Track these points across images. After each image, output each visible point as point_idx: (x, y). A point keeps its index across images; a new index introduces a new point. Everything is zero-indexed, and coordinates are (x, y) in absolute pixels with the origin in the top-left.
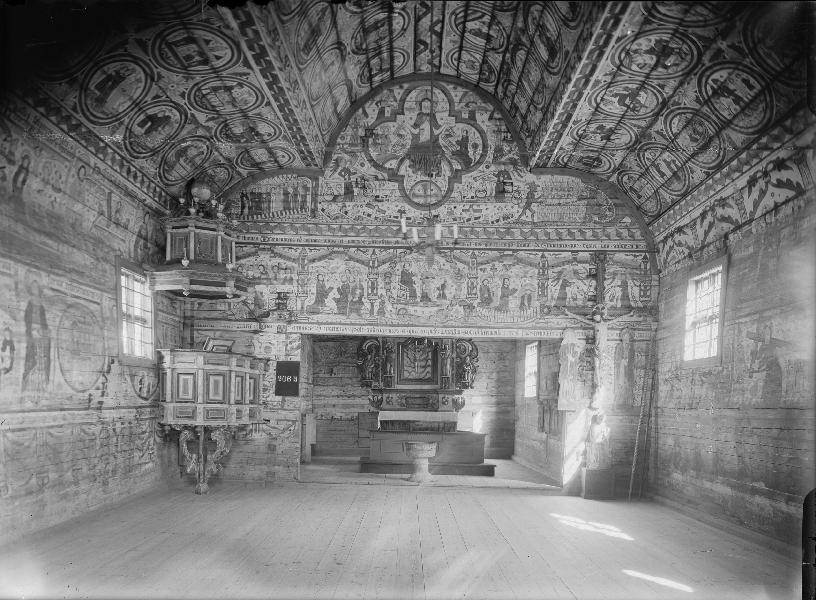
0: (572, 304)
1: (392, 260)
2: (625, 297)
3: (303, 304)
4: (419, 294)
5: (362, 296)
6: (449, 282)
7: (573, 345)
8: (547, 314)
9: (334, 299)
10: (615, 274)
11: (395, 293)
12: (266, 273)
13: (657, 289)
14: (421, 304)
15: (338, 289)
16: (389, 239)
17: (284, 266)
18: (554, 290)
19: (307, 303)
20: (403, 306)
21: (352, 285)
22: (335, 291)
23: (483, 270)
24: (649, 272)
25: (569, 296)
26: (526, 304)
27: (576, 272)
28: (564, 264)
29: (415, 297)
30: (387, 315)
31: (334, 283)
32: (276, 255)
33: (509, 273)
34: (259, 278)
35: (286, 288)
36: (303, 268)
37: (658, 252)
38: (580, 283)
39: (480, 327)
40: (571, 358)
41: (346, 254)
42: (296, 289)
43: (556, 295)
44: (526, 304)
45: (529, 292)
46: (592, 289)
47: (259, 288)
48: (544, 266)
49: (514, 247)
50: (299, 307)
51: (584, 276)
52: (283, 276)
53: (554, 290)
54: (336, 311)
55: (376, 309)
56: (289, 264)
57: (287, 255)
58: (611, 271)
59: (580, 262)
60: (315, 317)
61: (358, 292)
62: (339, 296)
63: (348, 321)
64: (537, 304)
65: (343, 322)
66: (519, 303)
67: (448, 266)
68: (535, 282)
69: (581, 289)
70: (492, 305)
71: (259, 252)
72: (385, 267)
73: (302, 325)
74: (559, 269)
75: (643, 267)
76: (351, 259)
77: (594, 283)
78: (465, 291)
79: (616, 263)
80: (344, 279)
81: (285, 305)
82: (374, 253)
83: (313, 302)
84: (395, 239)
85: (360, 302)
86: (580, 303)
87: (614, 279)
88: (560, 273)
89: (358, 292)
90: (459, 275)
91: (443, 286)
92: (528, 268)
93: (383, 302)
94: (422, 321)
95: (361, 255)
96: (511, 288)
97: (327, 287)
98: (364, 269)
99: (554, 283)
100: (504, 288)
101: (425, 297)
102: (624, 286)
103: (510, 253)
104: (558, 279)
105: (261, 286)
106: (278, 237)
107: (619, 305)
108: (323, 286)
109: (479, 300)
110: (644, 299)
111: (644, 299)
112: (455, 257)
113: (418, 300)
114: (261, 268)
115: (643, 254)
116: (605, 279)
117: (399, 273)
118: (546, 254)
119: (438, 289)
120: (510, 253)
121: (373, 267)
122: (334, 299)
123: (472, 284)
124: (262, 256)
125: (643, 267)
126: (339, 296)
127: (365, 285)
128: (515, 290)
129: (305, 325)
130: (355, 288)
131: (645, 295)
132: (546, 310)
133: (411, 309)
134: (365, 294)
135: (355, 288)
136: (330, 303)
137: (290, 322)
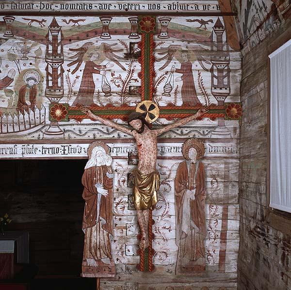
0: (104, 101)
2: (189, 88)
7: (104, 167)
8: (61, 118)
10: (170, 53)
13: (238, 76)
18: (73, 80)
24: (225, 48)
25: (98, 87)
26: (28, 103)
27: (107, 49)
28: (88, 36)
37: (236, 14)
38: (116, 67)
40: (101, 191)
43: (77, 87)
44: (28, 103)
46: (135, 76)
48: (55, 38)
51: (121, 55)
53: (73, 80)
58: (166, 44)
59: (116, 32)
64: (46, 102)
69: (116, 76)
74: (81, 44)
75: (215, 39)
77: (138, 66)
79: (173, 33)
86: (116, 99)
87: (170, 59)
88: (82, 50)
92: (30, 43)
99: (76, 65)
102: (186, 71)
104: (80, 61)
107: (180, 103)
110: (218, 91)
111: (218, 91)
115: (215, 19)
116: (154, 60)
118: (59, 19)
125: (215, 39)
131: (220, 86)
132: (58, 112)
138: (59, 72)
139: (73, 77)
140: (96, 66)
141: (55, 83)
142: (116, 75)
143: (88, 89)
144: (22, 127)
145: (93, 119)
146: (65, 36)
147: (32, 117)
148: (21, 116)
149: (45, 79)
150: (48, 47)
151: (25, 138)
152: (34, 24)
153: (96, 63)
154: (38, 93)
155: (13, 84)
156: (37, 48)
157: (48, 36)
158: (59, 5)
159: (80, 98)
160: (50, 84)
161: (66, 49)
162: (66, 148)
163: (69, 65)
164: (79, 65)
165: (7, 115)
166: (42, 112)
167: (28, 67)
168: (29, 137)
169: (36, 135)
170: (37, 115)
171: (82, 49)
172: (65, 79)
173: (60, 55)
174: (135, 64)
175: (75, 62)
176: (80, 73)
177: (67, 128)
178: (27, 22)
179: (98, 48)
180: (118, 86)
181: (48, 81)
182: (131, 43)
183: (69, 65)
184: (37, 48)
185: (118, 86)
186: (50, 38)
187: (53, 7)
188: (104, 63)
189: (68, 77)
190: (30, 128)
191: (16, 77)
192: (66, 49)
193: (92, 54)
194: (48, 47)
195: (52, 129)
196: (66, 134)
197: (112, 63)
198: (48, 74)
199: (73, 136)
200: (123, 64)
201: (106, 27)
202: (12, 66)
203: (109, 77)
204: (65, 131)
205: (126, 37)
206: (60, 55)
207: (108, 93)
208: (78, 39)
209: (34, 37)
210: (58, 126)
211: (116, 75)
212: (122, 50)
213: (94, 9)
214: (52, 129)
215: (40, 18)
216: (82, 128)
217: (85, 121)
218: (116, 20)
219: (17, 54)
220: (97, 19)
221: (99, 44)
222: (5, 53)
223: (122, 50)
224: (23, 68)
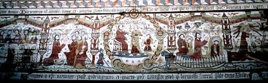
1: (110, 24)
3: (42, 57)
4: (130, 48)
5: (86, 50)
6: (154, 37)
9: (65, 53)
11: (112, 47)
12: (20, 35)
14: (131, 55)
15: (69, 46)
16: (109, 9)
17: (33, 30)
19: (45, 57)
20: (117, 57)
21: (79, 42)
22: (66, 47)
23: (180, 28)
25: (249, 44)
26: (216, 52)
27: (251, 26)
28: (241, 20)
29: (127, 49)
30: (105, 65)
31: (65, 41)
32: (27, 21)
33: (199, 29)
34: (14, 39)
35: (31, 46)
36: (45, 31)
38: (257, 34)
39: (180, 72)
41: (77, 20)
42: (38, 46)
43: (239, 44)
44: (216, 52)
45: (216, 43)
47: (12, 46)
48: (226, 22)
49: (202, 9)
50: (39, 60)
51: (258, 28)
52: (30, 37)
53: (236, 41)
54: (65, 62)
55: (96, 61)
56: (37, 28)
57: (37, 22)
59: (254, 18)
60: (49, 67)
61: (84, 47)
62: (69, 51)
63: (74, 70)
65: (70, 70)
66: (209, 50)
67: (152, 26)
68: (221, 35)
70: (189, 54)
71: (17, 21)
72: (105, 29)
73: (39, 74)
74: (238, 24)
76: (80, 23)
78: (165, 44)
80: (74, 38)
81: (29, 58)
82: (97, 18)
83: (49, 55)
84: (112, 8)
85: (85, 55)
86: (259, 49)
88: (239, 27)
89: (84, 47)
90: (160, 32)
91: (149, 42)
92: (214, 25)
93: (101, 55)
94: (133, 69)
95: (87, 21)
96: (202, 40)
97: (61, 44)
98: (89, 30)
99: (236, 35)
100: (198, 41)
101: (135, 50)
103: (199, 14)
104: (239, 32)
105: (15, 44)
106: (32, 10)
108: (58, 44)
109: (177, 51)
112: (157, 19)
113: (130, 52)
114: (17, 31)
117: (115, 32)
118: (226, 13)
119: (145, 43)
120: (199, 14)
121: (96, 29)
122: (65, 53)
123: (171, 38)
124: (18, 24)
126: (69, 51)
127: (89, 42)
128: (205, 42)
129: (41, 74)
130: (81, 45)
133: (124, 59)
134: (89, 49)
135: (81, 45)
136: (62, 56)
137: (30, 71)
138: (229, 37)
139: (236, 40)
140: (246, 34)
141: (228, 42)
142: (257, 38)
143: (244, 45)
144: (214, 64)
145: (250, 59)
146: (231, 21)
147: (218, 59)
148: (213, 59)
149: (223, 41)
150: (223, 26)
151: (216, 70)
152: (215, 16)
153: (247, 32)
154: (220, 47)
155: (208, 43)
156: (217, 26)
157: (222, 21)
158: (226, 7)
159: (241, 49)
160: (226, 43)
161: (231, 26)
162: (238, 74)
163: (234, 34)
164: (239, 34)
165: (206, 58)
166: (223, 56)
167: (214, 35)
168: (218, 69)
169: (222, 68)
170: (221, 58)
171: (239, 26)
172: (232, 41)
173: (229, 29)
174: (265, 32)
175: (236, 33)
176: (239, 38)
177: (237, 64)
178: (212, 15)
179: (246, 26)
180: (259, 43)
181: (224, 42)
182: (262, 24)
183: (234, 34)
184: (217, 26)
185: (259, 43)
186: (224, 22)
187: (223, 8)
188: (251, 32)
189: (234, 40)
190: (218, 65)
191: (209, 40)
192: (231, 26)
193: (244, 29)
194: (223, 26)
195: (229, 65)
196: (237, 67)
197: (255, 32)
198: (224, 38)
199: (240, 68)
200: (260, 32)
201: (249, 16)
202: (207, 35)
203: (254, 39)
204: (236, 66)
205: (259, 20)
206: (229, 29)
207: (255, 47)
208: (237, 22)
209: (215, 22)
210: (232, 63)
211: (257, 38)
212: (258, 26)
213: (242, 8)
214: (229, 65)
215: (217, 13)
216: (245, 64)
217: (247, 60)
218: (253, 13)
219: (208, 29)
220: (244, 13)
221: (247, 24)
222: (203, 29)
223: (258, 26)
224: (212, 36)
